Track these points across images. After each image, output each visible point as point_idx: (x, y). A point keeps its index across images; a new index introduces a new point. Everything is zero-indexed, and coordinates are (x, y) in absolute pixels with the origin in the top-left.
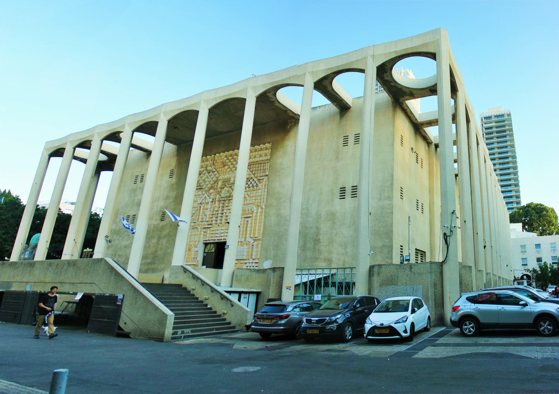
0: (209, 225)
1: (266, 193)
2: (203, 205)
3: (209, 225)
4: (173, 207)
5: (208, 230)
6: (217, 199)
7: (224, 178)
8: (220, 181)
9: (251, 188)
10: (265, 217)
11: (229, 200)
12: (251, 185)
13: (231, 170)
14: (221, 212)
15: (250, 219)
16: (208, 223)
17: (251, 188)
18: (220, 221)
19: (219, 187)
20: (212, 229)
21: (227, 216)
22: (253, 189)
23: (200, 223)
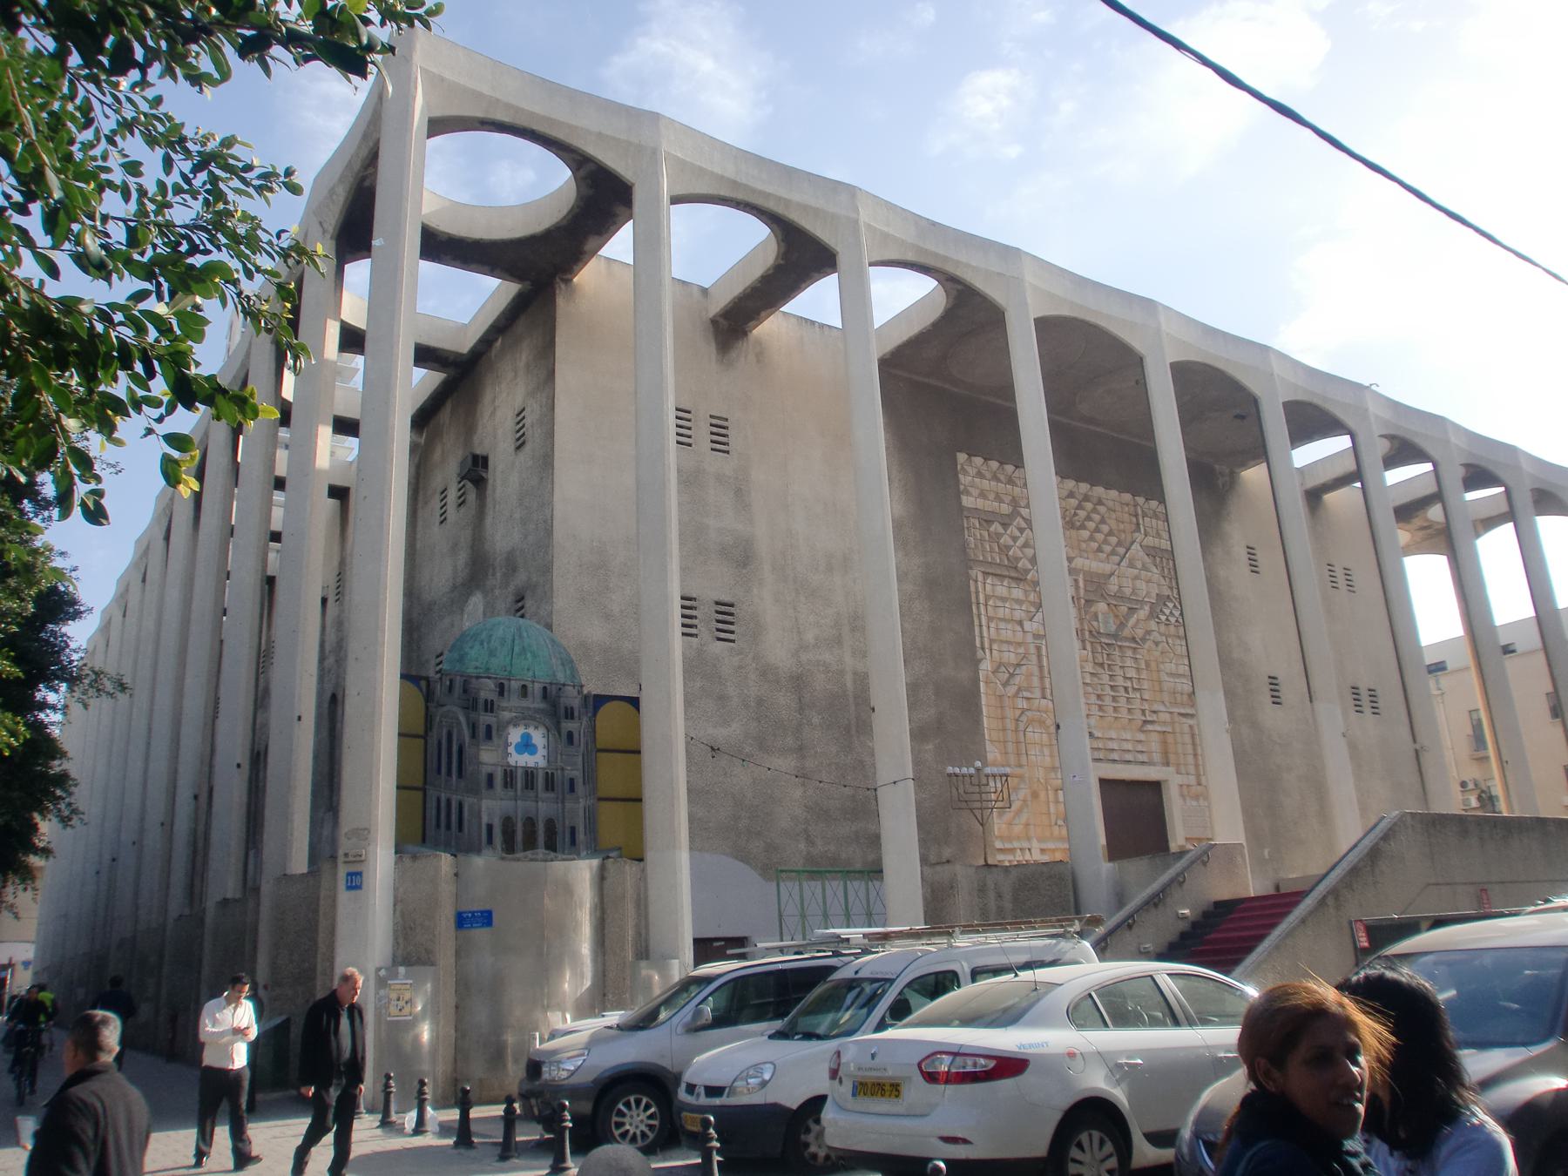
9: (1172, 629)
13: (1099, 550)
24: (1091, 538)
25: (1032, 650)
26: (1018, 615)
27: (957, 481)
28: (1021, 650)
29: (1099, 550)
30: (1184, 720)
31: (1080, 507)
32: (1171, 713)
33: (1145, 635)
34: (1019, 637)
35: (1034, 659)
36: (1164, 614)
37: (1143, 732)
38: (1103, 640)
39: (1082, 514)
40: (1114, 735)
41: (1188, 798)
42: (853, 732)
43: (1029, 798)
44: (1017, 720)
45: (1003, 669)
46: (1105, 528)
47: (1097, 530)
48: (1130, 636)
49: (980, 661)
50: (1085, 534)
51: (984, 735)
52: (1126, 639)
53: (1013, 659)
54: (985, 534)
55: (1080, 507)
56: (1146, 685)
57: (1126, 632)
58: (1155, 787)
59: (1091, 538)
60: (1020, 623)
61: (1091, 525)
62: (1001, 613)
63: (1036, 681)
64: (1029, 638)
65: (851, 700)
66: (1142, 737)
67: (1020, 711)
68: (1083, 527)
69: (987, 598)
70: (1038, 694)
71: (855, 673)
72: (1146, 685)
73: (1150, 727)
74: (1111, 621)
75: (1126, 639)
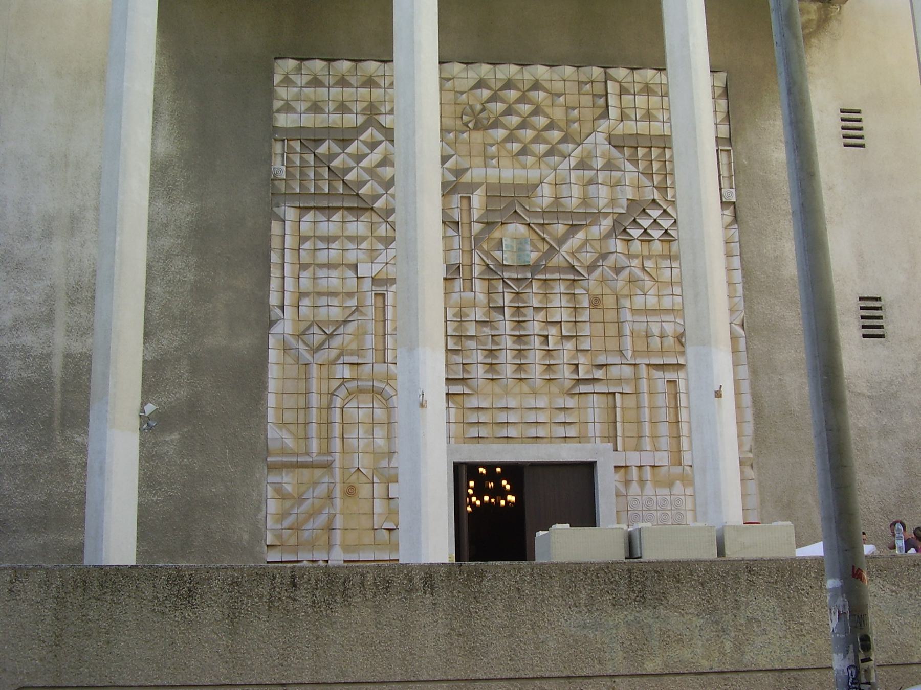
4: (191, 277)
6: (477, 271)
7: (493, 180)
9: (657, 247)
10: (754, 372)
11: (546, 280)
12: (656, 234)
14: (513, 330)
15: (682, 374)
17: (657, 247)
18: (515, 371)
19: (476, 215)
20: (473, 402)
21: (549, 350)
22: (666, 252)
24: (510, 138)
25: (369, 299)
26: (351, 257)
27: (270, 93)
28: (353, 302)
29: (524, 152)
30: (658, 374)
31: (494, 98)
32: (635, 365)
33: (597, 260)
34: (351, 284)
35: (370, 312)
36: (640, 226)
38: (506, 275)
39: (500, 107)
40: (512, 404)
41: (649, 485)
42: (56, 423)
43: (338, 493)
44: (332, 394)
45: (316, 329)
46: (542, 121)
47: (523, 125)
48: (566, 265)
49: (272, 323)
50: (501, 133)
51: (265, 416)
52: (558, 269)
53: (336, 313)
54: (310, 158)
55: (494, 98)
56: (586, 330)
57: (556, 261)
58: (589, 467)
59: (510, 138)
60: (355, 267)
61: (515, 120)
62: (322, 257)
63: (369, 342)
64: (367, 285)
65: (58, 387)
66: (570, 403)
67: (338, 383)
68: (496, 125)
69: (302, 239)
70: (370, 357)
71: (67, 356)
72: (586, 330)
73: (583, 388)
75: (558, 269)
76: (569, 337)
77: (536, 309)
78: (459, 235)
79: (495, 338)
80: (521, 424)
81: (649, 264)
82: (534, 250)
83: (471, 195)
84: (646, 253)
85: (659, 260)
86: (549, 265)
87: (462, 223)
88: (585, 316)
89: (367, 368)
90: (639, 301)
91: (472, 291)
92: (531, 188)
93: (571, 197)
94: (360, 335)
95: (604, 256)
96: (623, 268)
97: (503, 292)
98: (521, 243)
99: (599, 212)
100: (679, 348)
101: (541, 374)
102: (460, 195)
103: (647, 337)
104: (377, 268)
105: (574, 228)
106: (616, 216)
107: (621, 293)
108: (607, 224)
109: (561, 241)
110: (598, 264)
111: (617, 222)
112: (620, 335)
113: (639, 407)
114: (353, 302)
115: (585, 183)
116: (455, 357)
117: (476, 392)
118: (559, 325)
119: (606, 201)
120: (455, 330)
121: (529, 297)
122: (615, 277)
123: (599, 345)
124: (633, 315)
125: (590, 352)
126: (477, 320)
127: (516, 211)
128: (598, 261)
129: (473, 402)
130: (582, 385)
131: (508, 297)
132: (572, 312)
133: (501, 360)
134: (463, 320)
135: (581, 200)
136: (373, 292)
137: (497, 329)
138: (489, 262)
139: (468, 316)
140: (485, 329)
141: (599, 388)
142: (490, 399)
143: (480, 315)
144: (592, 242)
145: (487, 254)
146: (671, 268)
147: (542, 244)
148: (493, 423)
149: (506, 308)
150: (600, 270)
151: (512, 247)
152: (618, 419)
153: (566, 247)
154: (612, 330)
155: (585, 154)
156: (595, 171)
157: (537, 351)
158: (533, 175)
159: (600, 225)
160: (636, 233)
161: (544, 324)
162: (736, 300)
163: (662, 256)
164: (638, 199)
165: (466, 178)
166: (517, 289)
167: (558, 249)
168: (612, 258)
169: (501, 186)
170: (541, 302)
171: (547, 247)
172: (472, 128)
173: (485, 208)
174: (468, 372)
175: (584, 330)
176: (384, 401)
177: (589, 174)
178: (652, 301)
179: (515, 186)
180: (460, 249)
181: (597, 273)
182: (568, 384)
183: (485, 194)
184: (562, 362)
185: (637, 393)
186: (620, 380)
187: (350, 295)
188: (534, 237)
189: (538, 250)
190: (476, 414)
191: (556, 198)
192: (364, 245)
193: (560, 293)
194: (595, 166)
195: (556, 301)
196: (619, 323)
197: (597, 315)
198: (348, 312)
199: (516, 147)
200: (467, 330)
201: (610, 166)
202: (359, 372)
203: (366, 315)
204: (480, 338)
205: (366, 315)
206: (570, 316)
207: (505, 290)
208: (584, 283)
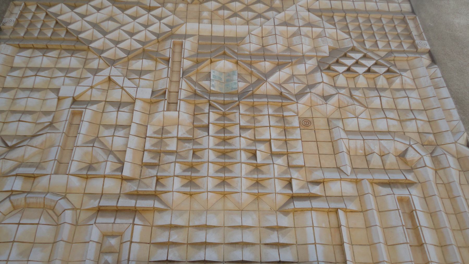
0: (131, 195)
1: (450, 103)
2: (94, 107)
3: (131, 195)
5: (137, 221)
6: (183, 95)
8: (191, 39)
9: (362, 81)
13: (235, 15)
16: (130, 187)
22: (372, 85)
23: (75, 182)
33: (304, 89)
34: (52, 104)
37: (286, 213)
48: (274, 92)
54: (42, 16)
57: (264, 88)
62: (28, 83)
64: (67, 103)
70: (50, 167)
73: (298, 204)
74: (236, 77)
76: (279, 155)
77: (242, 128)
78: (168, 68)
79: (198, 154)
80: (223, 246)
81: (355, 93)
82: (242, 81)
83: (184, 41)
84: (352, 85)
85: (367, 92)
86: (257, 92)
87: (173, 62)
88: (297, 134)
89: (44, 181)
90: (352, 124)
91: (177, 111)
92: (239, 39)
93: (277, 43)
94: (44, 149)
95: (312, 86)
96: (331, 96)
97: (209, 113)
98: (229, 76)
99: (303, 56)
100: (403, 167)
101: (248, 188)
102: (172, 40)
103: (366, 155)
104: (80, 90)
105: (279, 66)
106: (319, 59)
107: (332, 117)
108: (311, 64)
109: (268, 75)
110: (306, 91)
111: (320, 62)
112: (335, 152)
113: (368, 227)
114: (48, 119)
115: (289, 36)
116: (150, 170)
117: (168, 208)
118: (268, 143)
119: (309, 48)
120: (153, 145)
121: (235, 116)
122: (325, 101)
123: (312, 161)
124: (347, 135)
125: (304, 168)
126: (179, 136)
127: (224, 54)
128: (306, 90)
129: (165, 219)
130: (296, 201)
131: (213, 117)
132: (281, 132)
133: (203, 172)
134: (164, 136)
135: (286, 48)
136: (71, 109)
137: (200, 144)
138: (197, 88)
139: (170, 133)
140: (186, 144)
141: (316, 204)
142: (186, 216)
143: (182, 133)
144: (299, 77)
145: (195, 83)
146: (380, 97)
147: (250, 77)
148: (188, 244)
149: (211, 126)
150: (309, 95)
151: (221, 79)
152: (346, 239)
153: (273, 79)
154: (326, 148)
155: (287, 18)
156: (297, 28)
157: (243, 165)
158: (242, 29)
159: (305, 64)
160: (341, 69)
161: (252, 142)
162: (455, 123)
163: (369, 88)
164: (339, 48)
165: (181, 30)
166: (223, 110)
167: (265, 79)
168: (320, 87)
169: (212, 38)
170: (248, 122)
171: (254, 80)
172: (190, 3)
173: (196, 51)
174: (163, 186)
175: (295, 147)
176: (55, 218)
177: (292, 30)
178: (365, 124)
179: (225, 38)
180: (168, 77)
181: (305, 99)
182: (281, 200)
183: (196, 42)
184: (272, 176)
185: (363, 211)
186: (341, 198)
187: (47, 113)
188: (243, 72)
189: (245, 81)
190: (167, 233)
191: (263, 46)
192: (73, 74)
193: (269, 115)
194: (297, 24)
195: (265, 121)
196: (333, 142)
197: (308, 134)
198: (40, 127)
199: (227, 13)
200: (167, 145)
201: (310, 24)
202: (35, 184)
203: (58, 129)
204: (180, 153)
205: (58, 129)
206: (279, 134)
207: (210, 110)
208: (294, 107)
